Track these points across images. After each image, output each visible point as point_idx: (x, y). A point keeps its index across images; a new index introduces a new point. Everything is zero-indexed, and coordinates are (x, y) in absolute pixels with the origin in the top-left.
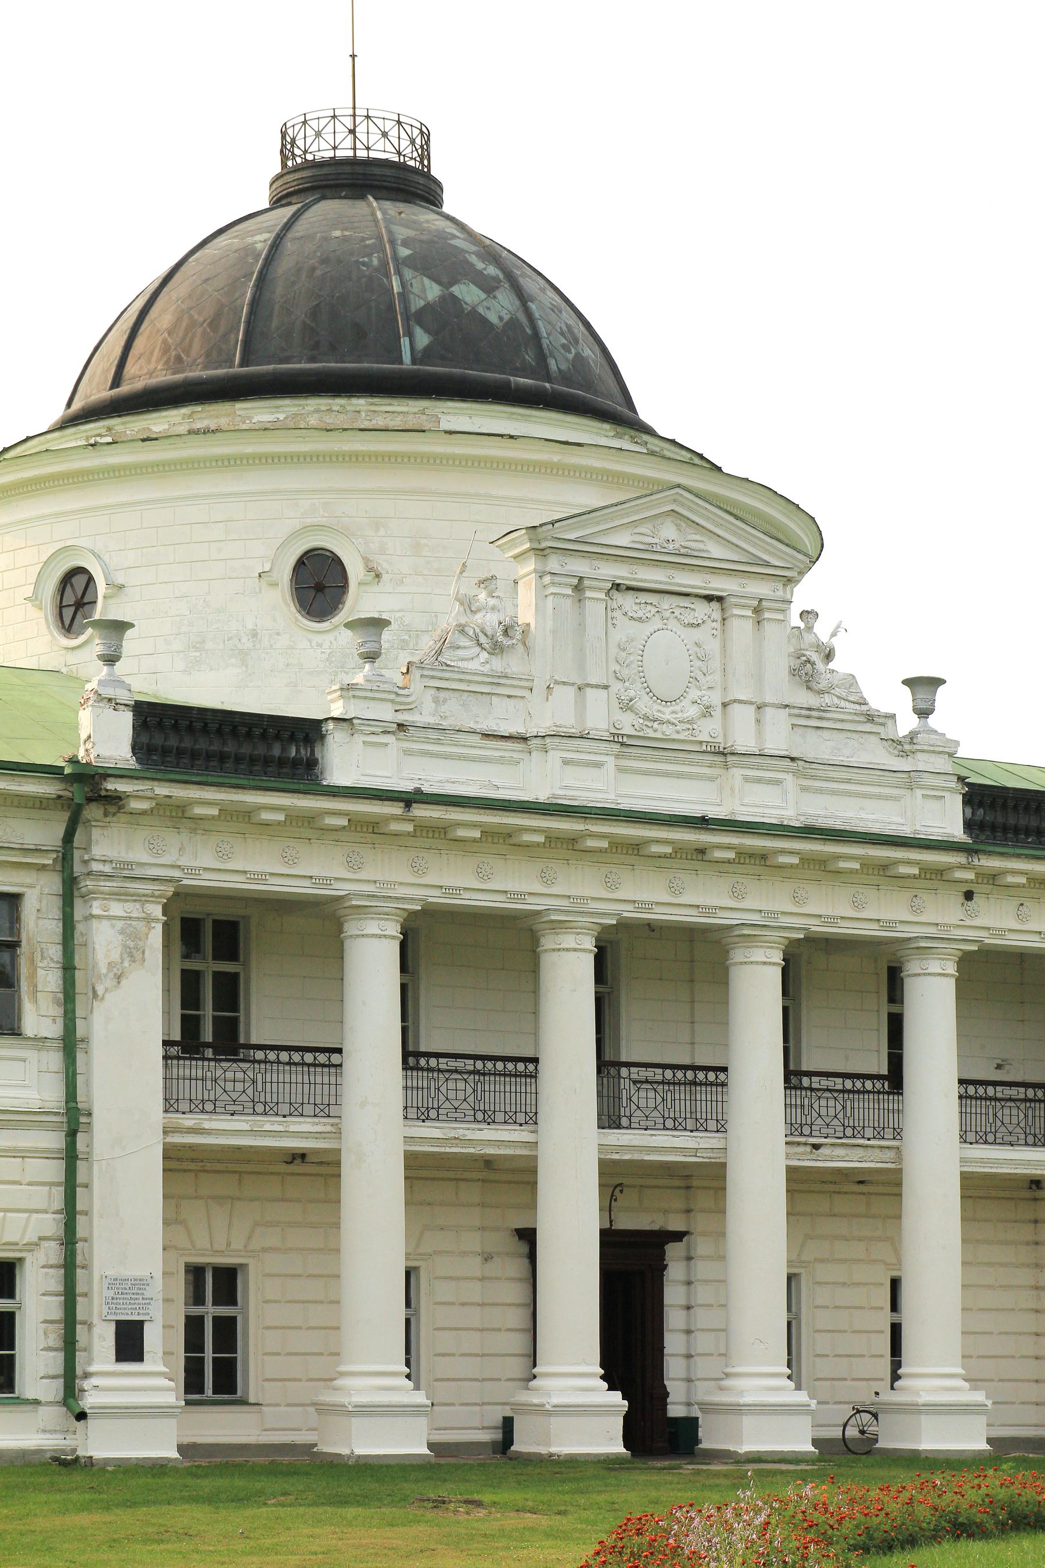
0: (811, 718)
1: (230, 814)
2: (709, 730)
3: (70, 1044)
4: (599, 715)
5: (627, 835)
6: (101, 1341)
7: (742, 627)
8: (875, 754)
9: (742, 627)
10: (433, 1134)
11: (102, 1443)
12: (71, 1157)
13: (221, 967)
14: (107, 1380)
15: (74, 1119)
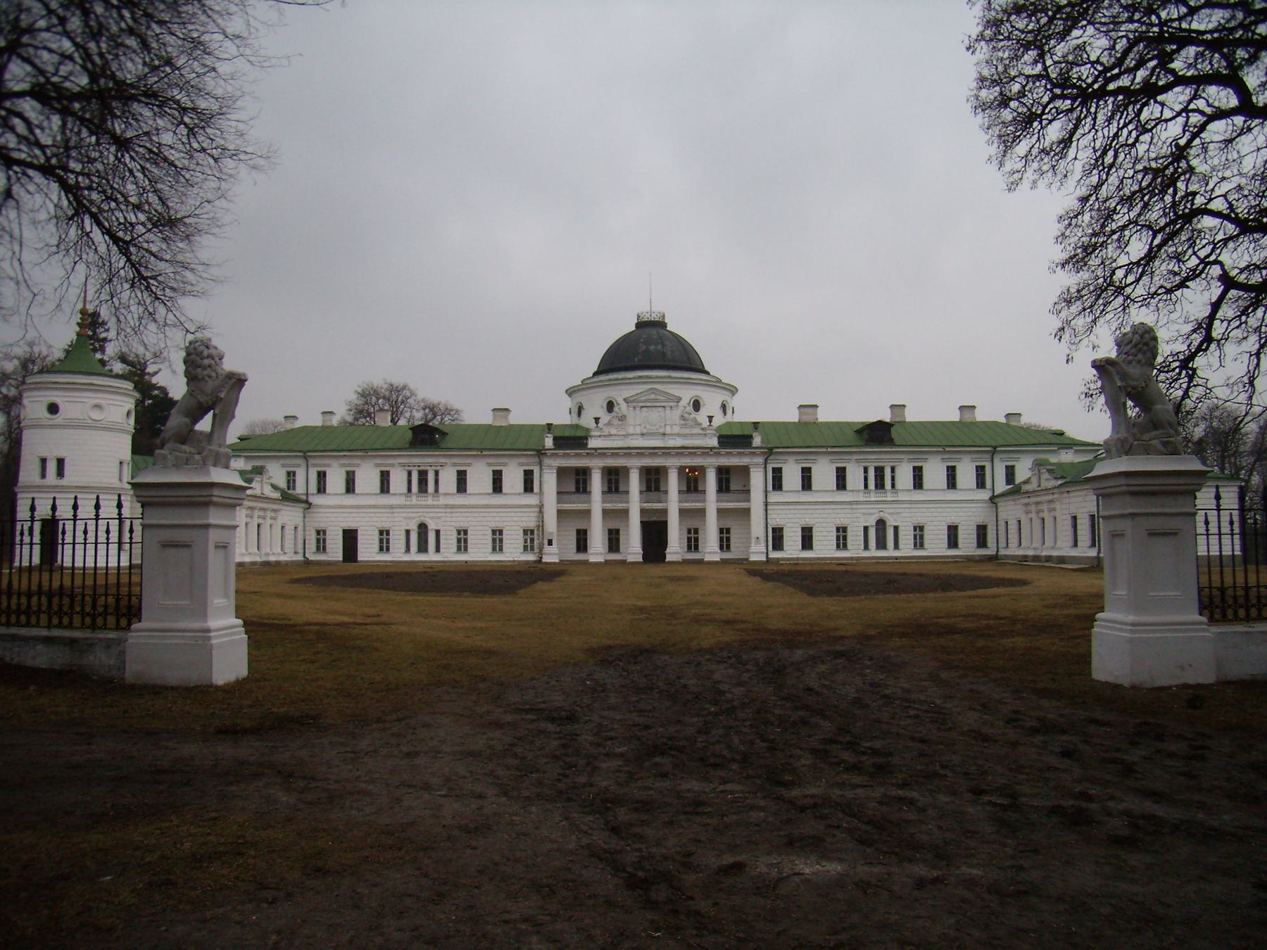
0: (683, 426)
1: (577, 454)
2: (661, 431)
3: (541, 493)
4: (638, 430)
5: (641, 452)
6: (546, 542)
7: (668, 411)
8: (697, 431)
9: (668, 411)
10: (609, 506)
11: (546, 559)
12: (541, 512)
13: (577, 480)
14: (547, 549)
15: (541, 508)
